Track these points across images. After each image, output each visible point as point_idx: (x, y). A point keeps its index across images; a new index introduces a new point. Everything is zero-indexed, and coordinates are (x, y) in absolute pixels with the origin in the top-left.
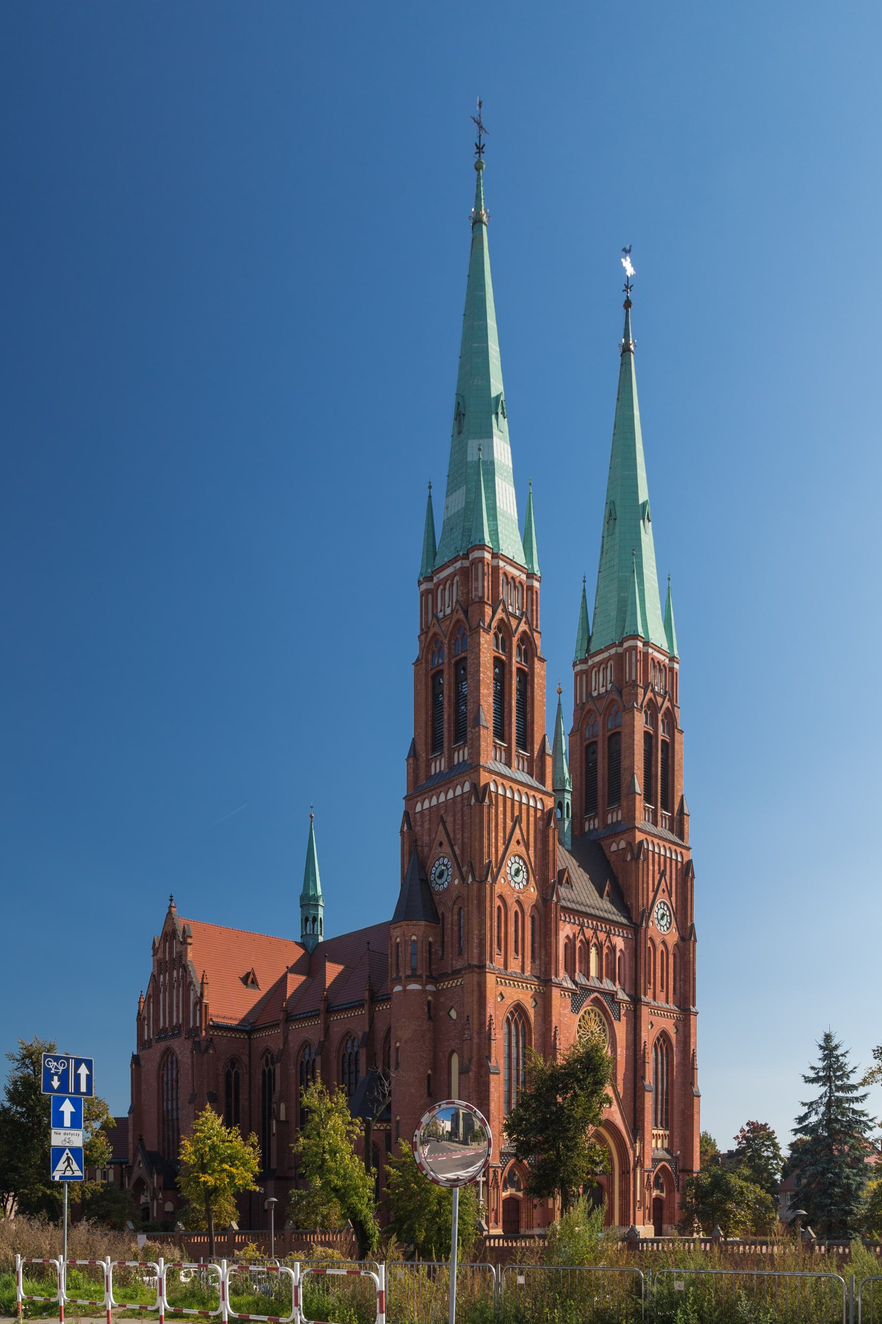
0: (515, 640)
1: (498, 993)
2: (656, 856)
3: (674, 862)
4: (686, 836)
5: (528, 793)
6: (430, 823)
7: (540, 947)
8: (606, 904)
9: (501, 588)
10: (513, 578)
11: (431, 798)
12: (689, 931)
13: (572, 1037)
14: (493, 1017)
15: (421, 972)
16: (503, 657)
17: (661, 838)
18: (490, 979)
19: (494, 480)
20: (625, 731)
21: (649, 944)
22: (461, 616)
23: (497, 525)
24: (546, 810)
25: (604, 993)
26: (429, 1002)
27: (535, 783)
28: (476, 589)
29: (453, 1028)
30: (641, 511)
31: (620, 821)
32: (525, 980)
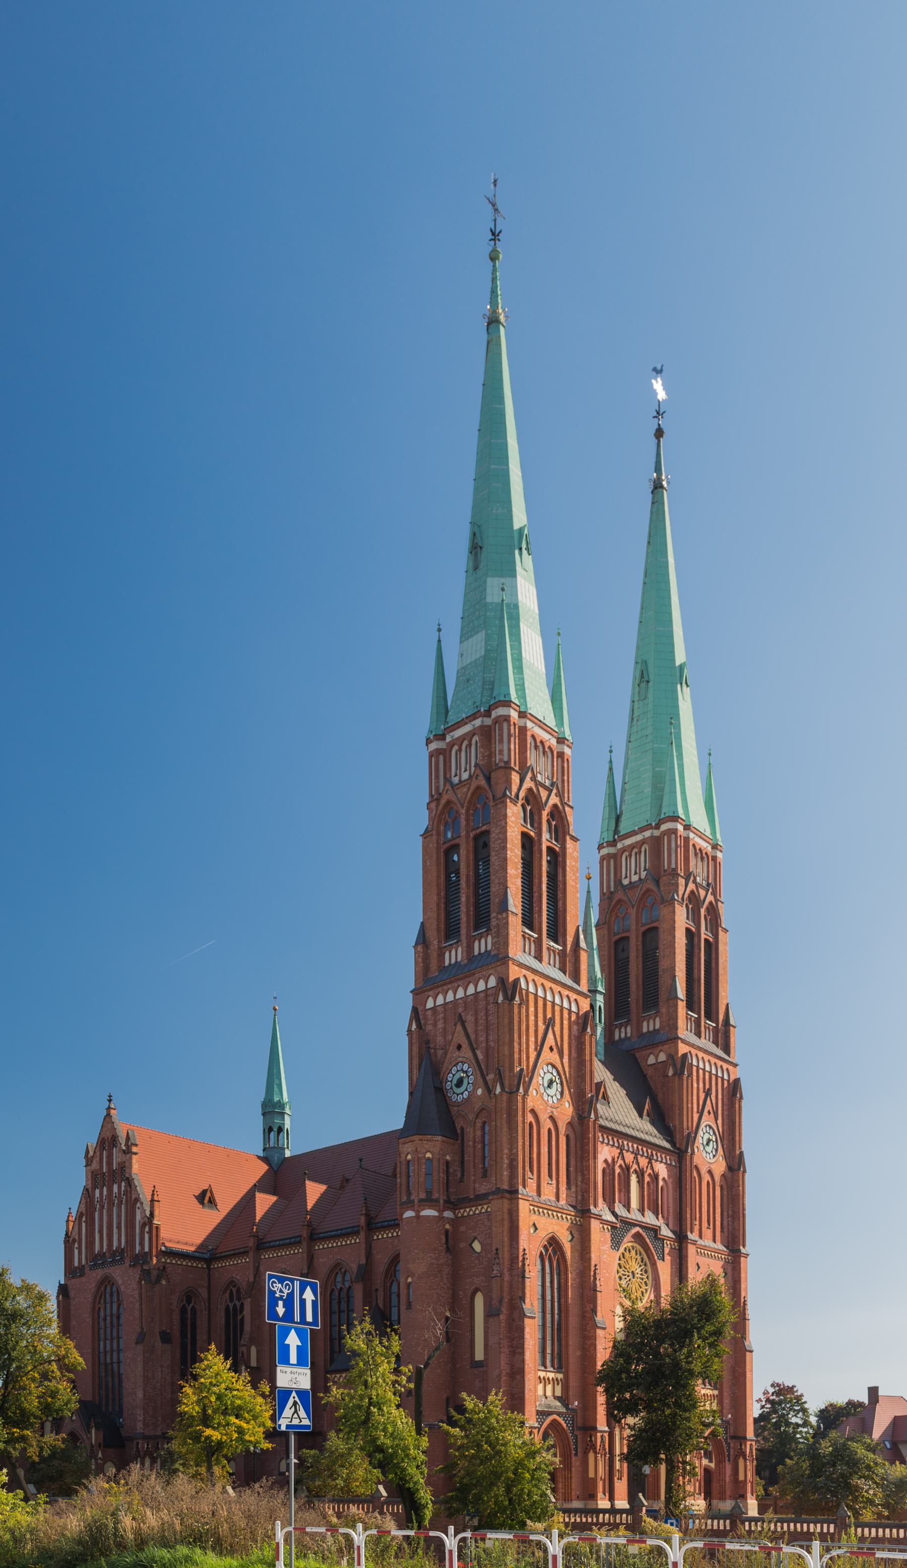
0: (545, 814)
1: (531, 1223)
2: (701, 1071)
3: (720, 1080)
4: (732, 1051)
5: (562, 992)
6: (445, 1023)
7: (576, 1172)
8: (649, 1127)
9: (528, 752)
10: (542, 742)
11: (447, 992)
12: (737, 1161)
13: (612, 1278)
14: (527, 1252)
15: (437, 1195)
16: (532, 834)
17: (706, 1052)
18: (524, 1207)
19: (519, 627)
20: (663, 927)
21: (695, 1174)
22: (483, 783)
23: (523, 679)
24: (581, 1013)
25: (645, 1228)
26: (447, 1231)
27: (569, 982)
28: (501, 752)
29: (477, 1262)
30: (678, 674)
31: (658, 1030)
32: (560, 1210)
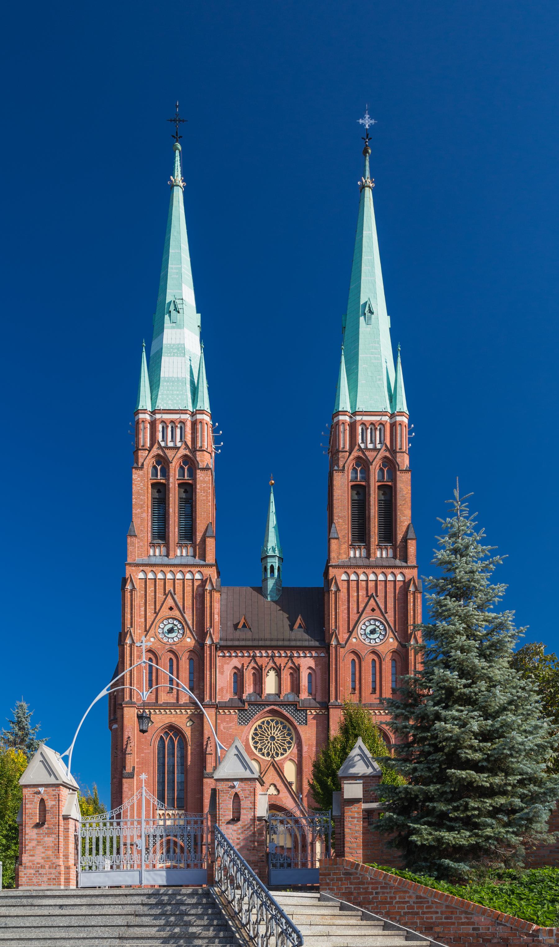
27: (197, 561)
